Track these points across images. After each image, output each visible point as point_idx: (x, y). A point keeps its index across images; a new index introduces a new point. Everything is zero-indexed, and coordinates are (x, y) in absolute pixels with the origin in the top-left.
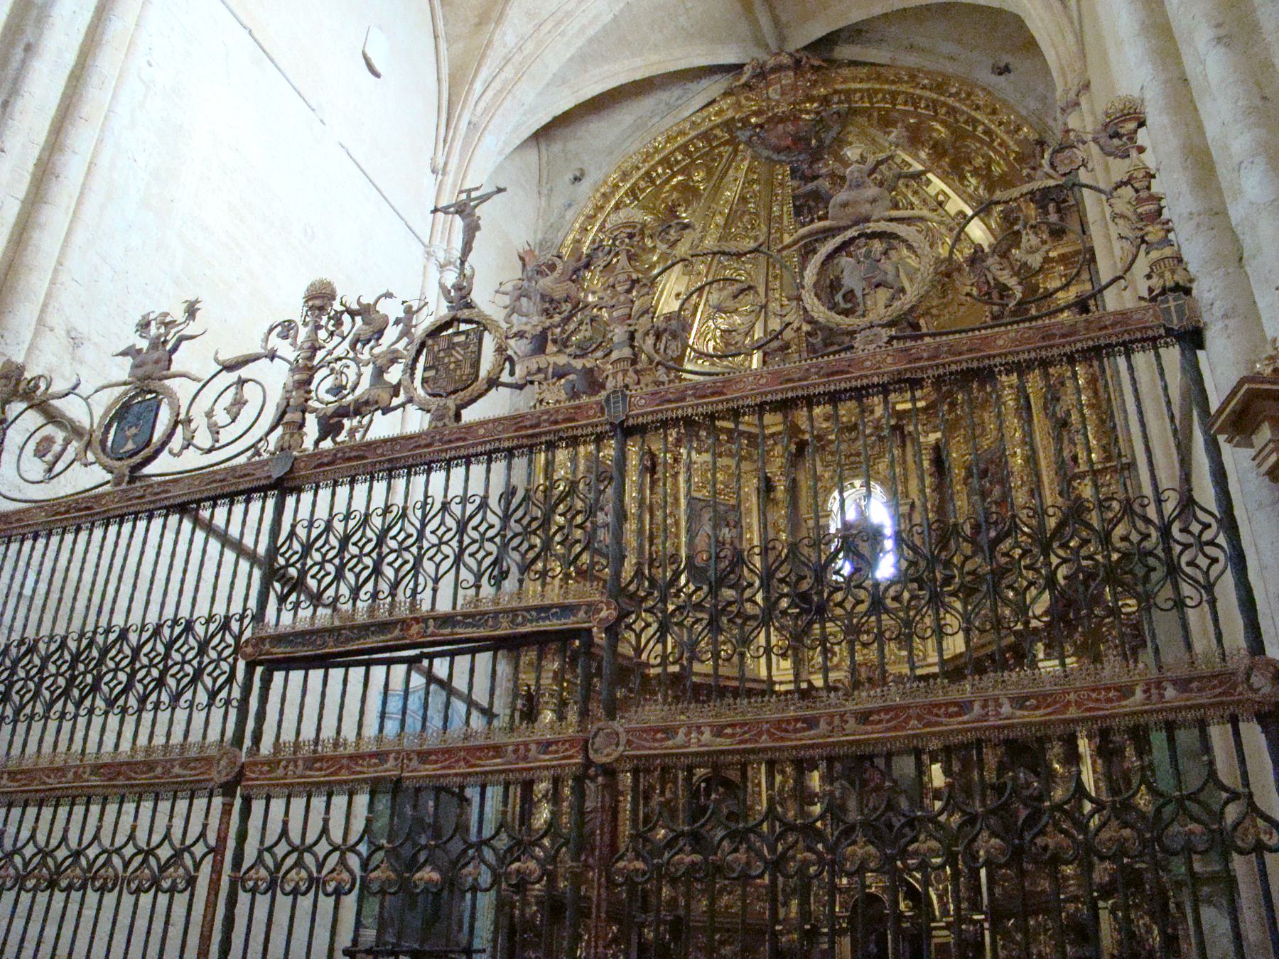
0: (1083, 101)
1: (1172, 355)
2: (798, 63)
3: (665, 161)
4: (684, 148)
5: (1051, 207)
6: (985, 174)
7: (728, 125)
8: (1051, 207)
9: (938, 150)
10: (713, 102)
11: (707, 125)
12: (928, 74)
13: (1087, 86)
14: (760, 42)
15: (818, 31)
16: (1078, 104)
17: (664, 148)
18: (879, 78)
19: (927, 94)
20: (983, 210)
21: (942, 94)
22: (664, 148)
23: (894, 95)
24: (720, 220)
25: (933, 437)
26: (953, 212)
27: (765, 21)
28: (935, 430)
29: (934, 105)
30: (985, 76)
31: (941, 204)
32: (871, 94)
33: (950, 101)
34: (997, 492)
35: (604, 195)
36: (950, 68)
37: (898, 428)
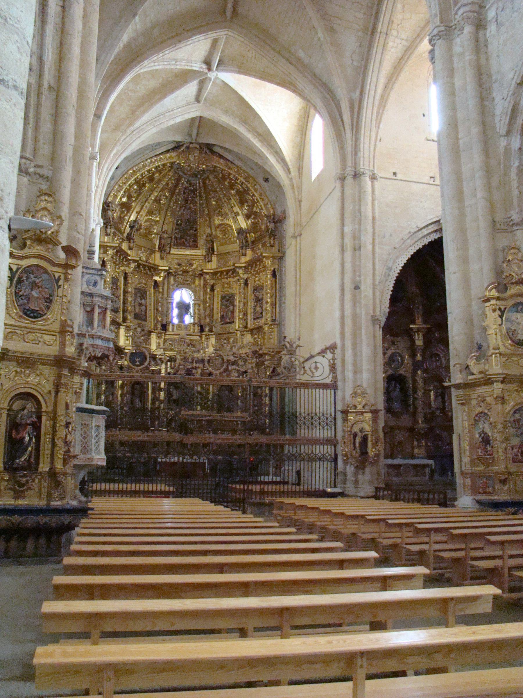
0: (298, 238)
1: (333, 391)
2: (201, 148)
3: (149, 171)
4: (156, 168)
5: (272, 238)
6: (251, 207)
7: (172, 164)
8: (272, 238)
9: (238, 193)
10: (168, 151)
11: (165, 162)
12: (244, 171)
13: (300, 235)
14: (190, 135)
15: (211, 141)
16: (296, 237)
17: (149, 166)
18: (227, 166)
19: (242, 179)
20: (247, 217)
21: (246, 181)
22: (149, 166)
23: (230, 174)
24: (159, 190)
25: (212, 282)
26: (235, 211)
27: (195, 132)
28: (213, 279)
29: (243, 183)
30: (262, 181)
31: (232, 207)
32: (223, 170)
33: (249, 185)
34: (231, 308)
35: (126, 178)
36: (251, 172)
37: (201, 275)
